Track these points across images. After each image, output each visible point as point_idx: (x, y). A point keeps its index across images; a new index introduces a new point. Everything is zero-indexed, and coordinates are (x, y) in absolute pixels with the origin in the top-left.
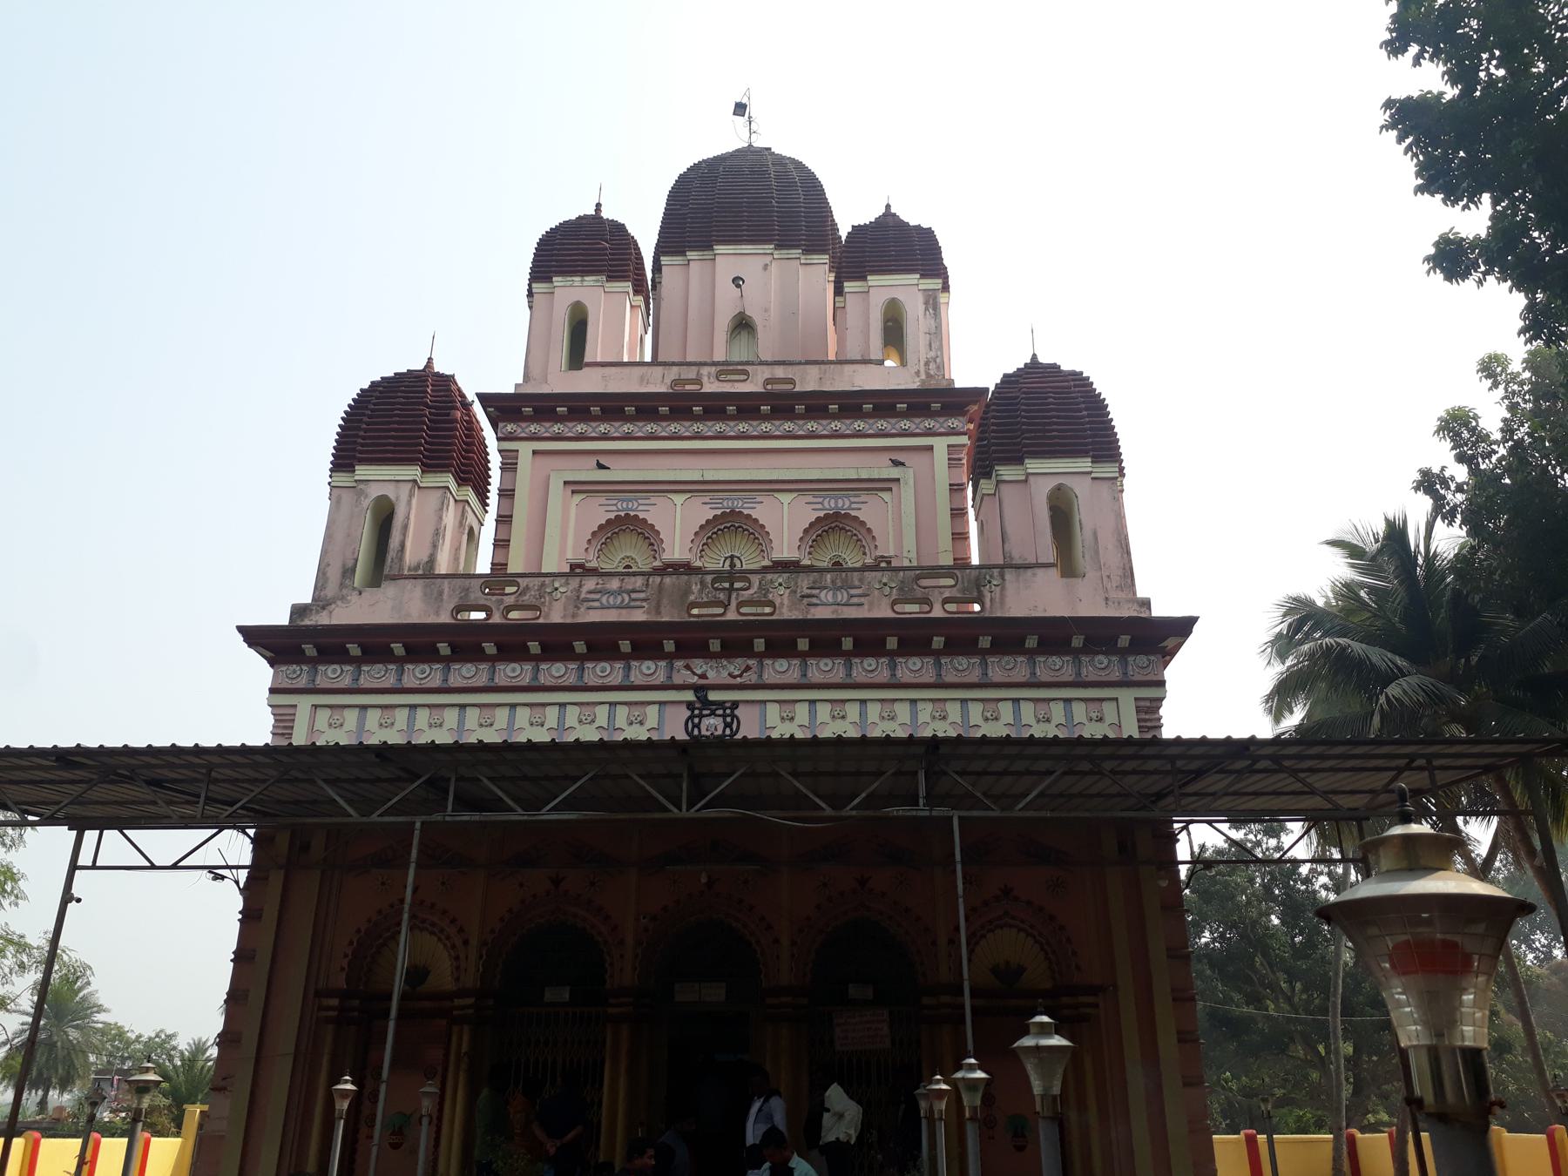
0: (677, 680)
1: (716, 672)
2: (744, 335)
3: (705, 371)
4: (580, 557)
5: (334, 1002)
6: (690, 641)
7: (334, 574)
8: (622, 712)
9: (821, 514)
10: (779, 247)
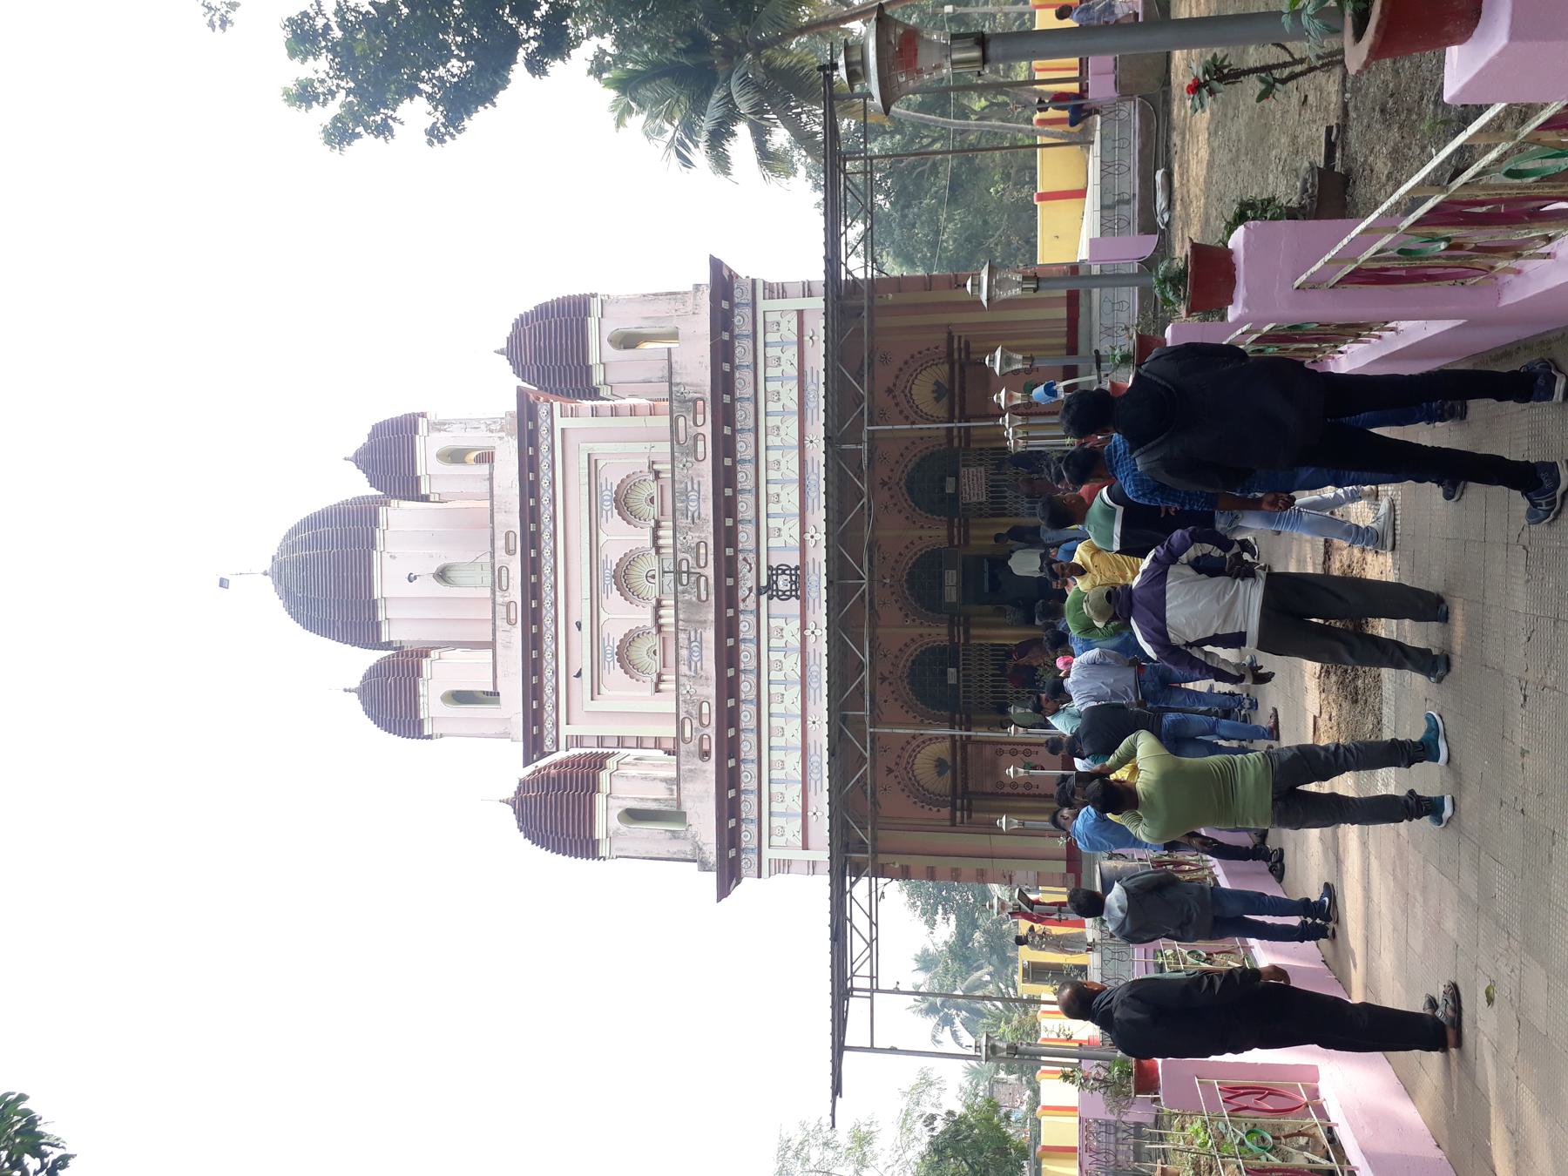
0: (754, 607)
1: (747, 581)
2: (449, 574)
3: (499, 600)
4: (650, 686)
5: (958, 814)
6: (727, 598)
7: (675, 847)
8: (774, 643)
10: (373, 545)
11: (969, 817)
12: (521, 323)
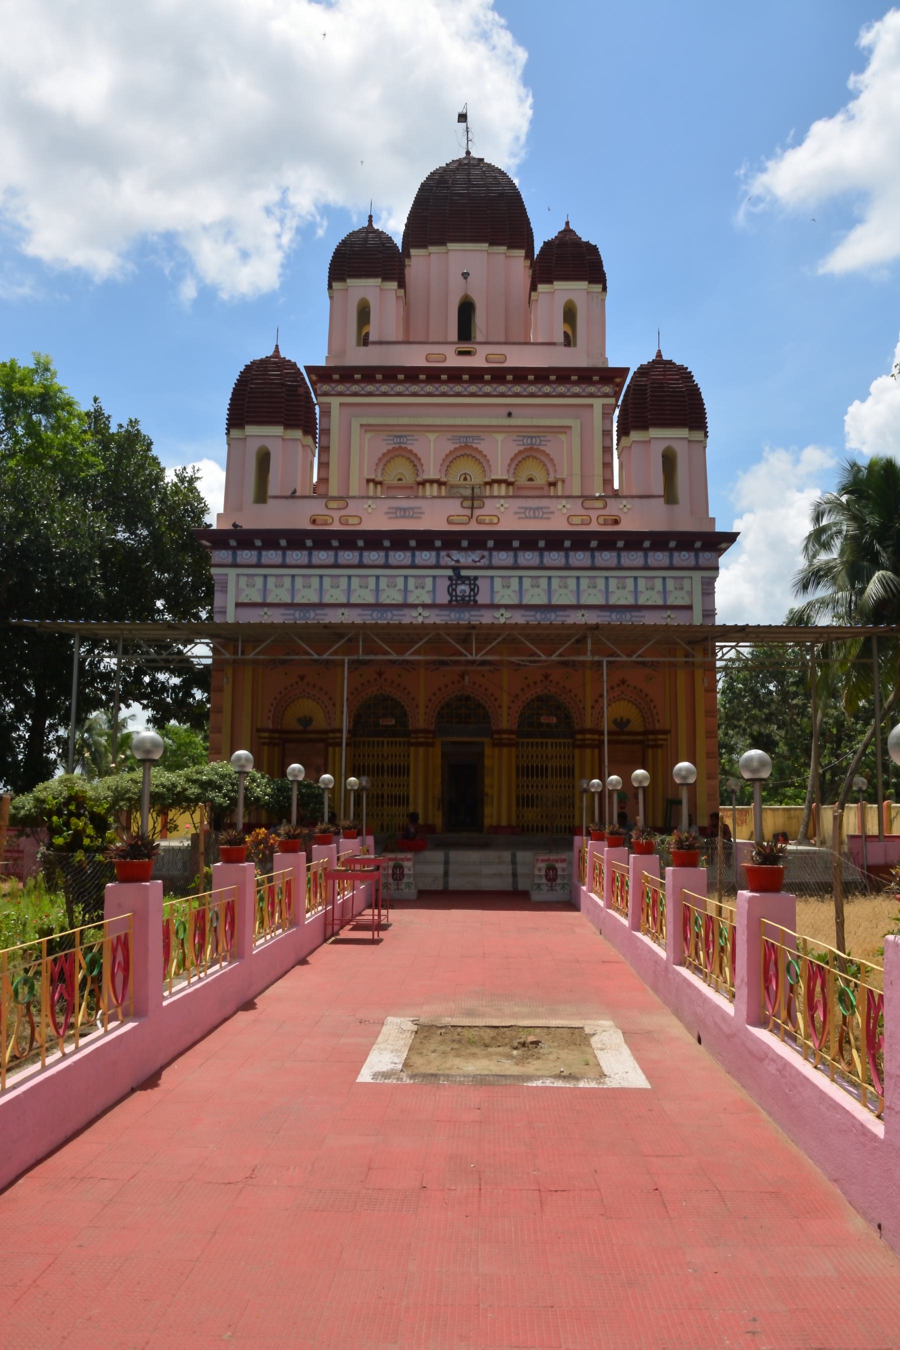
4: (372, 477)
5: (266, 735)
9: (522, 448)
11: (264, 744)
12: (684, 375)
